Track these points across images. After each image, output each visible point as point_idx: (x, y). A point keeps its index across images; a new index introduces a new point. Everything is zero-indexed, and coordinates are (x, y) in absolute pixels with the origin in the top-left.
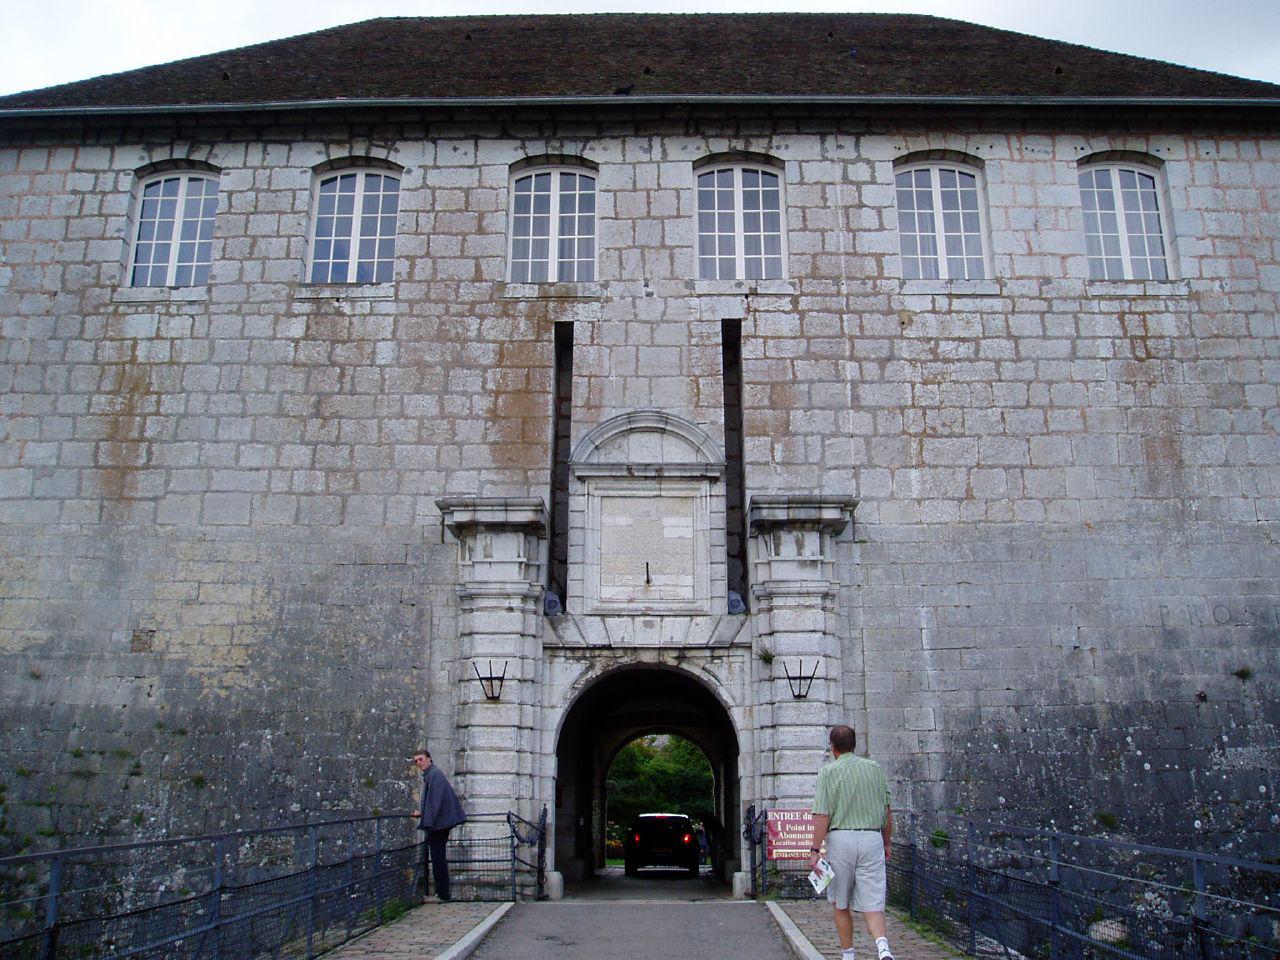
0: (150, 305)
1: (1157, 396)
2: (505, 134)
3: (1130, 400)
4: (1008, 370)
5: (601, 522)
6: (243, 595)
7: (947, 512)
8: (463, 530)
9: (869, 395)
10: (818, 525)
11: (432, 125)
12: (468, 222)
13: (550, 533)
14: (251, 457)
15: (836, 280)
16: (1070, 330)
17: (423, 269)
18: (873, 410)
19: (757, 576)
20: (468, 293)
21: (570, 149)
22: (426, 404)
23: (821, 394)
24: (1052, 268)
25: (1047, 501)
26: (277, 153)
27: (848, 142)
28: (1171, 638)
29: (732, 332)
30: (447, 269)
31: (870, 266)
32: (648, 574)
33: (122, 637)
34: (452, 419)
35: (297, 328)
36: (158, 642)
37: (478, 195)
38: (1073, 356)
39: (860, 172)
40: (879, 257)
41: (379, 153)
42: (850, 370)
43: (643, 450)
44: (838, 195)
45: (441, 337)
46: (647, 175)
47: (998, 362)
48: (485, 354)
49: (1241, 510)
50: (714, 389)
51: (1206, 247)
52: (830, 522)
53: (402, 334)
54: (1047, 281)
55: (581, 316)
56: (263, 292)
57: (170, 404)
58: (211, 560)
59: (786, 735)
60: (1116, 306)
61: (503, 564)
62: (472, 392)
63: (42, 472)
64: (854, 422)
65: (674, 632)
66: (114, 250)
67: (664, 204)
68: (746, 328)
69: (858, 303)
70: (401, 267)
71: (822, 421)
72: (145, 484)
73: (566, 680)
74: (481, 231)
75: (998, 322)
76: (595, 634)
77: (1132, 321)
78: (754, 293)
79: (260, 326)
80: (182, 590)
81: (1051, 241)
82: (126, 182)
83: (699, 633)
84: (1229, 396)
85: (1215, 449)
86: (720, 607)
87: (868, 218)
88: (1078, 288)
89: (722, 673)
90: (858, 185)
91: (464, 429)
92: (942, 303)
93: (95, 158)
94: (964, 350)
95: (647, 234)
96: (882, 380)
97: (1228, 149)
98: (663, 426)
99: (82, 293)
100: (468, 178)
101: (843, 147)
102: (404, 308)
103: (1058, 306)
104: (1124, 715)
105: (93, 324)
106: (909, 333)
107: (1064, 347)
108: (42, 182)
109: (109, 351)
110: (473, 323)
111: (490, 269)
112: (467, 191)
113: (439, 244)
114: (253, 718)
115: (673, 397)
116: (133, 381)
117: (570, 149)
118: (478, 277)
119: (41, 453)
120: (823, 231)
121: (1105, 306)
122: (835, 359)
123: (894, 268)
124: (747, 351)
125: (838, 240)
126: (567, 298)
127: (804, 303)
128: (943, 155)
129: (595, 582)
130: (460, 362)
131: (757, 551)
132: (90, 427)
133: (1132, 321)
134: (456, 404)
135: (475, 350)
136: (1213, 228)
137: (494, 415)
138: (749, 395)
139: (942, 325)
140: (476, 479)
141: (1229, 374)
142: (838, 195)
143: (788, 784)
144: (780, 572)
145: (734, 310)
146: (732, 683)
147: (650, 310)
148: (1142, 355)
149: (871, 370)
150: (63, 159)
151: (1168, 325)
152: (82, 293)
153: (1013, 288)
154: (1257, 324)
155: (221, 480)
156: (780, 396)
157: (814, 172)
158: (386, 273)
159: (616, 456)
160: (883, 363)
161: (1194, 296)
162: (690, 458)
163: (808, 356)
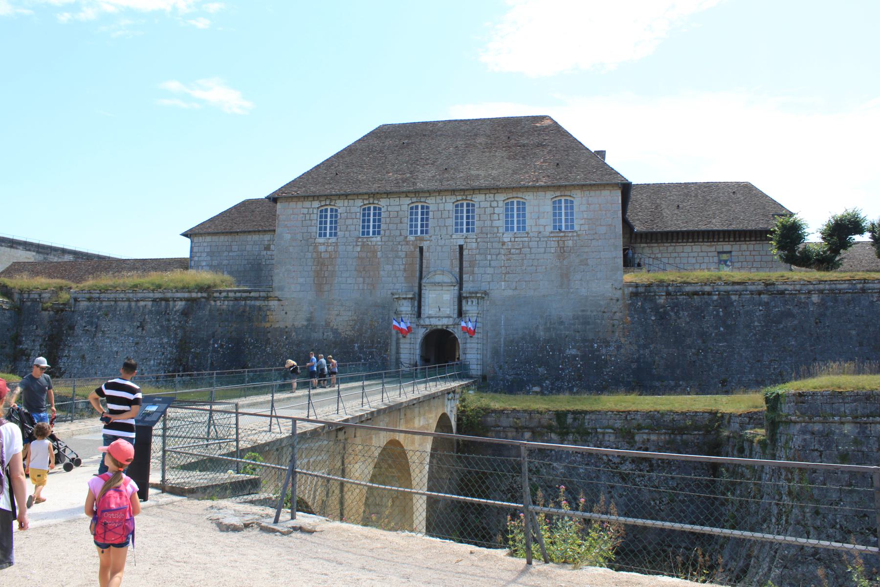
0: (324, 244)
2: (407, 196)
3: (558, 264)
4: (528, 256)
5: (430, 296)
6: (350, 313)
7: (509, 293)
8: (398, 299)
10: (478, 298)
12: (397, 220)
13: (418, 299)
17: (387, 233)
18: (494, 267)
19: (464, 309)
20: (398, 239)
22: (389, 267)
24: (542, 229)
25: (535, 290)
28: (562, 323)
29: (461, 247)
30: (393, 233)
31: (495, 230)
32: (439, 307)
33: (323, 323)
35: (359, 249)
36: (331, 324)
37: (400, 213)
39: (494, 204)
40: (498, 227)
42: (489, 257)
43: (438, 278)
45: (392, 250)
48: (402, 254)
49: (583, 292)
51: (582, 222)
52: (482, 296)
55: (425, 245)
58: (342, 305)
60: (557, 239)
64: (490, 270)
65: (445, 321)
66: (313, 229)
67: (445, 214)
68: (464, 247)
69: (492, 240)
70: (382, 232)
71: (481, 270)
72: (326, 288)
73: (421, 333)
74: (401, 223)
75: (526, 244)
76: (427, 322)
78: (466, 238)
79: (350, 248)
80: (337, 312)
81: (542, 221)
82: (315, 211)
86: (456, 316)
87: (496, 217)
88: (548, 234)
89: (456, 330)
91: (398, 273)
92: (513, 239)
94: (517, 251)
99: (307, 240)
100: (398, 209)
104: (547, 341)
107: (542, 250)
110: (400, 247)
111: (404, 233)
113: (391, 226)
114: (352, 341)
118: (401, 235)
119: (301, 280)
122: (486, 255)
123: (501, 230)
124: (465, 252)
125: (488, 223)
126: (422, 240)
127: (479, 240)
129: (429, 309)
130: (397, 257)
131: (464, 302)
135: (400, 253)
136: (585, 216)
137: (405, 270)
138: (465, 264)
142: (489, 211)
143: (468, 356)
145: (461, 242)
146: (458, 333)
147: (441, 242)
148: (562, 252)
149: (494, 257)
151: (570, 243)
152: (307, 240)
153: (531, 234)
154: (594, 243)
156: (472, 264)
157: (483, 204)
158: (379, 233)
160: (497, 255)
161: (578, 236)
163: (479, 254)
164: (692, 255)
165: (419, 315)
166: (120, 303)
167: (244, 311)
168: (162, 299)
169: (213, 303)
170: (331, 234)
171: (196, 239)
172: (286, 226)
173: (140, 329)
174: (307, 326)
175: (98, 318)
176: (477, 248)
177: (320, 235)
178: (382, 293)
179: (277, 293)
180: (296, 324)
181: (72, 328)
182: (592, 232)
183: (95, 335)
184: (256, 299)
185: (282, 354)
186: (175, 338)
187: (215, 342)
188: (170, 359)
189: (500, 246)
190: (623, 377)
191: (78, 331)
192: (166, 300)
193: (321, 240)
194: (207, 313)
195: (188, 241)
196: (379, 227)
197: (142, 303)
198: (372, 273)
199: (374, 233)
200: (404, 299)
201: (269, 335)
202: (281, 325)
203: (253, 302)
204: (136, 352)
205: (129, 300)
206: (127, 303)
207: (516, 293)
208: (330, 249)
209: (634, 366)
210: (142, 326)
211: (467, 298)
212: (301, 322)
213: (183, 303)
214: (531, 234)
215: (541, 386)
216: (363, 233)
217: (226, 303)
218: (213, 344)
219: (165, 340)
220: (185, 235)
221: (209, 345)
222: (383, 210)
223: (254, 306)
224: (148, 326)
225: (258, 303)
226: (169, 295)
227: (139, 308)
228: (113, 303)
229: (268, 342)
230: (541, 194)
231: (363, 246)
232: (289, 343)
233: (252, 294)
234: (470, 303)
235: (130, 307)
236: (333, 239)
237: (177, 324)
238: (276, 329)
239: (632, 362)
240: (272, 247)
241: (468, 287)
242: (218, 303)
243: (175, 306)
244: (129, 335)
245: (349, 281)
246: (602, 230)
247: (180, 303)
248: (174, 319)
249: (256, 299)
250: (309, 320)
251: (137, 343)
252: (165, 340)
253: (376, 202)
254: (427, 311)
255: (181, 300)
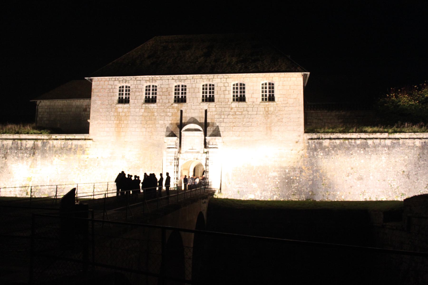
1: (269, 120)
3: (265, 121)
12: (166, 93)
15: (222, 102)
16: (256, 110)
18: (226, 123)
29: (206, 111)
30: (164, 101)
37: (169, 89)
38: (257, 114)
40: (228, 99)
47: (245, 115)
48: (170, 114)
51: (279, 96)
53: (158, 111)
54: (254, 102)
60: (264, 106)
74: (169, 95)
75: (245, 109)
77: (266, 108)
79: (137, 110)
87: (227, 92)
90: (226, 87)
94: (240, 113)
96: (227, 118)
99: (111, 105)
102: (158, 107)
103: (255, 106)
106: (232, 111)
107: (255, 113)
110: (168, 110)
112: (167, 88)
113: (163, 97)
118: (169, 102)
120: (220, 95)
121: (262, 106)
122: (220, 115)
125: (222, 96)
127: (217, 106)
133: (266, 108)
135: (169, 114)
136: (281, 93)
139: (237, 109)
142: (223, 89)
152: (111, 105)
154: (286, 108)
172: (98, 96)
173: (4, 159)
176: (216, 111)
182: (286, 102)
189: (230, 110)
190: (304, 190)
222: (158, 87)
239: (309, 181)
246: (291, 101)
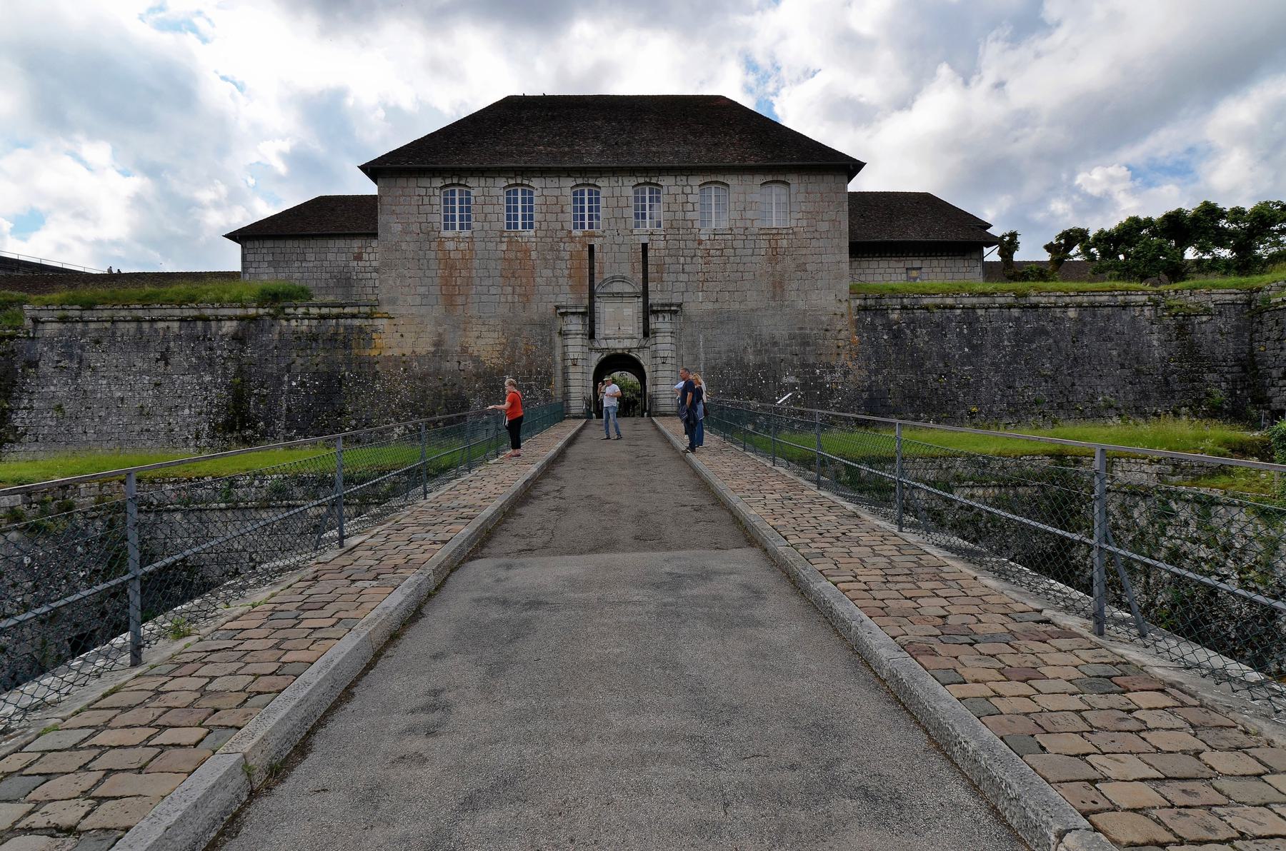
0: (453, 239)
1: (778, 267)
2: (569, 176)
5: (605, 310)
7: (710, 306)
9: (687, 268)
11: (544, 172)
13: (589, 315)
14: (493, 290)
17: (544, 226)
19: (652, 326)
20: (560, 234)
21: (591, 181)
22: (548, 273)
23: (672, 268)
24: (749, 224)
26: (490, 181)
27: (684, 178)
28: (775, 344)
29: (645, 246)
30: (552, 226)
32: (619, 324)
33: (458, 349)
34: (557, 277)
35: (504, 247)
36: (470, 350)
39: (688, 190)
41: (526, 182)
43: (617, 288)
44: (681, 198)
45: (552, 249)
46: (617, 192)
48: (566, 255)
49: (801, 305)
50: (639, 267)
52: (674, 310)
55: (597, 242)
56: (491, 234)
57: (464, 273)
59: (660, 374)
61: (575, 325)
62: (563, 268)
63: (424, 296)
64: (683, 277)
65: (627, 344)
67: (623, 202)
69: (685, 237)
70: (536, 225)
71: (673, 277)
72: (460, 300)
73: (596, 358)
76: (604, 346)
77: (773, 242)
79: (491, 246)
80: (477, 334)
82: (437, 192)
83: (635, 344)
84: (802, 267)
85: (794, 285)
86: (641, 336)
87: (690, 207)
93: (425, 182)
94: (718, 253)
95: (617, 213)
97: (812, 179)
98: (623, 280)
100: (557, 192)
101: (682, 180)
104: (760, 366)
105: (434, 245)
108: (407, 191)
109: (440, 255)
111: (567, 226)
113: (549, 216)
114: (502, 373)
115: (627, 272)
116: (449, 265)
117: (591, 181)
119: (422, 290)
123: (697, 225)
125: (680, 215)
126: (592, 236)
128: (716, 182)
130: (558, 258)
131: (652, 319)
132: (437, 281)
133: (773, 242)
134: (558, 272)
140: (566, 298)
141: (803, 260)
142: (681, 198)
143: (660, 388)
144: (658, 326)
146: (644, 359)
147: (619, 240)
148: (775, 255)
150: (413, 182)
153: (735, 231)
155: (484, 298)
156: (661, 268)
157: (672, 190)
158: (531, 226)
159: (608, 290)
160: (692, 258)
161: (794, 233)
162: (631, 290)
163: (669, 255)
164: (878, 271)
165: (592, 336)
166: (121, 325)
167: (336, 334)
168: (196, 319)
169: (284, 323)
170: (461, 227)
171: (249, 245)
172: (393, 212)
173: (162, 363)
174: (434, 354)
175: (82, 348)
176: (666, 248)
177: (446, 228)
178: (542, 307)
179: (386, 308)
180: (418, 350)
181: (33, 364)
183: (78, 375)
184: (354, 316)
185: (398, 393)
186: (225, 375)
187: (293, 378)
188: (217, 406)
191: (46, 368)
192: (206, 319)
193: (449, 233)
194: (276, 337)
195: (236, 248)
196: (531, 217)
197: (161, 325)
198: (524, 280)
199: (524, 226)
200: (573, 313)
201: (378, 367)
202: (396, 352)
203: (349, 321)
204: (157, 397)
205: (138, 320)
206: (134, 325)
207: (717, 306)
208: (463, 246)
209: (865, 395)
210: (165, 358)
211: (656, 312)
212: (425, 347)
213: (235, 323)
214: (735, 231)
215: (755, 423)
216: (509, 226)
217: (306, 322)
218: (290, 382)
219: (208, 378)
220: (232, 236)
221: (282, 384)
222: (535, 193)
223: (352, 327)
224: (175, 360)
225: (357, 322)
226: (208, 312)
227: (156, 331)
228: (108, 325)
229: (376, 375)
230: (748, 178)
231: (510, 242)
232: (409, 377)
233: (347, 310)
234: (661, 319)
235: (140, 330)
236: (466, 233)
237: (225, 354)
238: (388, 358)
240: (365, 256)
241: (655, 298)
242: (293, 323)
243: (220, 328)
244: (142, 372)
245: (493, 290)
247: (228, 323)
248: (220, 347)
249: (354, 316)
250: (438, 344)
251: (156, 385)
252: (208, 378)
253: (526, 182)
254: (602, 331)
255: (230, 319)
